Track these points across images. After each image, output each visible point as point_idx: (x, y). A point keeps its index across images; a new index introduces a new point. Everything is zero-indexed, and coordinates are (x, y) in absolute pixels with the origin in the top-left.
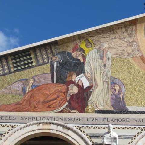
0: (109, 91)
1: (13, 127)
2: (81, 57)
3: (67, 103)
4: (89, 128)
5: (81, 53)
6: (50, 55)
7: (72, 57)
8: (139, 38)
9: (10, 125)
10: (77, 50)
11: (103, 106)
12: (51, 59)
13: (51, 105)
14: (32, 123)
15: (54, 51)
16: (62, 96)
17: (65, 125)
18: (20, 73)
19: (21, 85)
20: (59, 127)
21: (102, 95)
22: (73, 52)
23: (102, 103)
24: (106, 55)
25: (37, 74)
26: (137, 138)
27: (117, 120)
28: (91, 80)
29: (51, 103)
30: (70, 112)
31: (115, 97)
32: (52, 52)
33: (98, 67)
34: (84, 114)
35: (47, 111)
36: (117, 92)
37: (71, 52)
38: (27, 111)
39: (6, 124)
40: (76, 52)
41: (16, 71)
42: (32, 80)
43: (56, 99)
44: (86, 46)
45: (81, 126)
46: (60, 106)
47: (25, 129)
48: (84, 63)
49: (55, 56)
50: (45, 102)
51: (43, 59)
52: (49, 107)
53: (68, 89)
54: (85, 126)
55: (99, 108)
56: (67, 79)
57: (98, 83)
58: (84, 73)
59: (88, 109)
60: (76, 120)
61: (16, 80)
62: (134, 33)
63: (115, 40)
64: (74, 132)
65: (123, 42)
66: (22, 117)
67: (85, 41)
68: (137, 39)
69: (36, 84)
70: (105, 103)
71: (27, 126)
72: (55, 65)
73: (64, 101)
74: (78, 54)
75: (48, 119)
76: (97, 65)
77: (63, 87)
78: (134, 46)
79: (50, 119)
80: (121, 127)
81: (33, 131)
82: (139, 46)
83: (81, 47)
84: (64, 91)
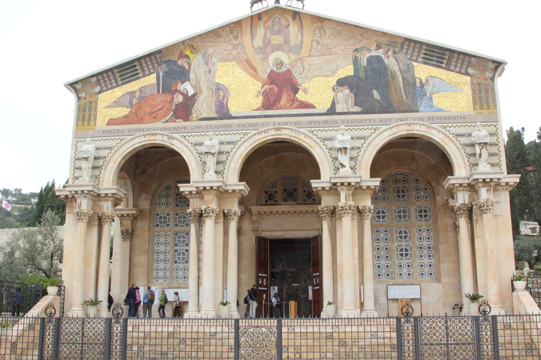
0: (213, 97)
1: (121, 140)
2: (187, 64)
3: (172, 113)
4: (194, 136)
5: (187, 60)
6: (156, 65)
7: (178, 65)
8: (244, 39)
9: (119, 138)
10: (182, 57)
11: (208, 113)
12: (157, 69)
13: (157, 115)
14: (139, 135)
15: (159, 60)
16: (167, 105)
17: (170, 134)
18: (128, 85)
19: (128, 98)
20: (164, 137)
21: (206, 102)
22: (178, 59)
23: (206, 110)
24: (211, 60)
25: (143, 85)
26: (239, 143)
27: (220, 126)
28: (196, 87)
29: (157, 113)
30: (175, 122)
31: (219, 103)
32: (158, 62)
33: (202, 74)
34: (188, 122)
35: (154, 122)
36: (221, 98)
37: (176, 59)
38: (134, 123)
39: (115, 137)
40: (181, 60)
41: (123, 84)
42: (138, 91)
43: (161, 109)
44: (192, 52)
45: (185, 134)
46: (165, 116)
47: (132, 141)
48: (189, 70)
49: (160, 65)
50: (151, 113)
51: (149, 70)
52: (155, 118)
53: (173, 98)
54: (189, 134)
55: (203, 115)
56: (173, 88)
57: (203, 91)
58: (189, 80)
59: (193, 118)
60: (180, 129)
61: (124, 93)
62: (240, 34)
63: (220, 44)
64: (179, 140)
65: (229, 45)
66: (130, 131)
67: (190, 47)
68: (243, 41)
69: (143, 95)
70: (209, 110)
71: (134, 138)
72: (161, 74)
73: (169, 110)
74: (183, 61)
75: (154, 130)
76: (202, 71)
77: (168, 97)
78: (239, 48)
79: (156, 130)
80: (224, 134)
81: (140, 143)
82: (244, 48)
83: (186, 54)
84: (169, 100)
